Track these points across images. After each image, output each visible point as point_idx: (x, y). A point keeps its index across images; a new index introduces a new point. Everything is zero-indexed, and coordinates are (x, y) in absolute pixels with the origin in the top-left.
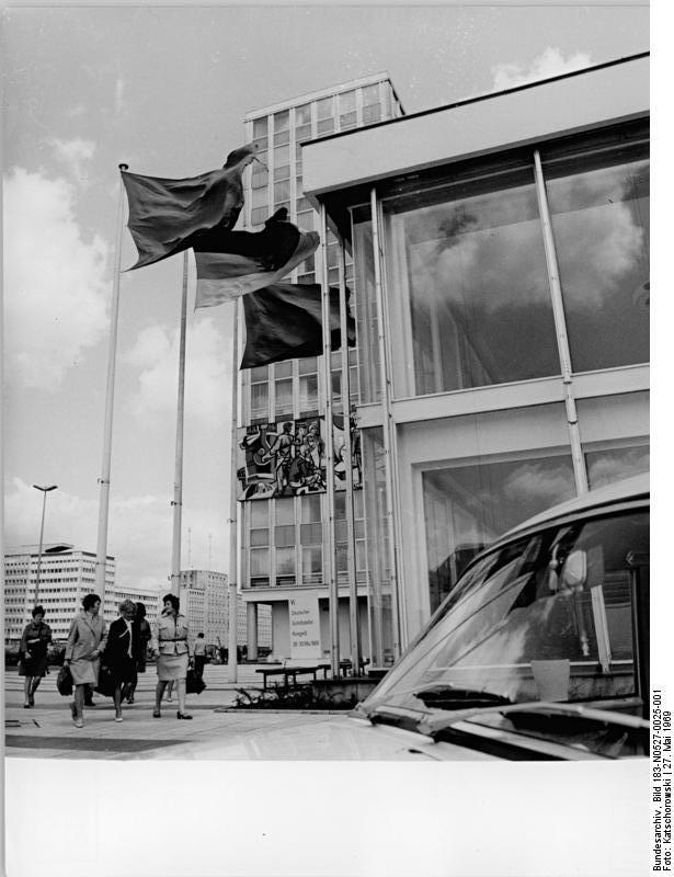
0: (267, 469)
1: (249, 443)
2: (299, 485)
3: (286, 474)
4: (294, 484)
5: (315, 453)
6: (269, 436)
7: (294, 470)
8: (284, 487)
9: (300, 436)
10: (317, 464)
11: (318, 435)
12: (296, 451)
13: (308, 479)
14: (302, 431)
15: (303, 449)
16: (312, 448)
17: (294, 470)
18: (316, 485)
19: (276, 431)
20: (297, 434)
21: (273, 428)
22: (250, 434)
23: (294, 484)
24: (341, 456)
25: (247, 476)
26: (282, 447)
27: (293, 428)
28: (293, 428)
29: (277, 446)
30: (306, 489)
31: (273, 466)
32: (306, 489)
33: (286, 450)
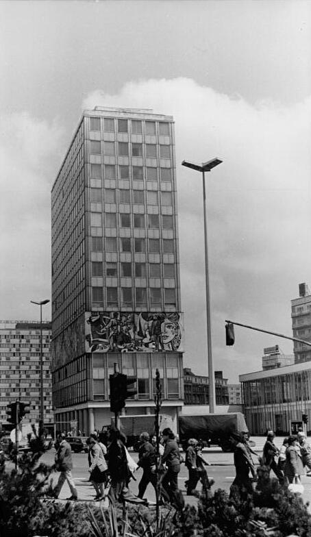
0: (104, 337)
1: (93, 320)
2: (122, 347)
3: (115, 341)
4: (119, 347)
5: (131, 331)
6: (104, 319)
7: (120, 338)
8: (114, 348)
9: (123, 321)
10: (133, 337)
11: (133, 322)
12: (121, 329)
13: (128, 344)
14: (124, 319)
15: (124, 328)
16: (129, 329)
17: (120, 338)
18: (132, 349)
19: (109, 316)
20: (121, 319)
21: (107, 314)
22: (93, 316)
23: (119, 347)
24: (146, 335)
25: (92, 340)
26: (112, 326)
27: (119, 316)
28: (119, 316)
29: (110, 324)
30: (126, 350)
31: (107, 335)
32: (126, 350)
33: (115, 328)
